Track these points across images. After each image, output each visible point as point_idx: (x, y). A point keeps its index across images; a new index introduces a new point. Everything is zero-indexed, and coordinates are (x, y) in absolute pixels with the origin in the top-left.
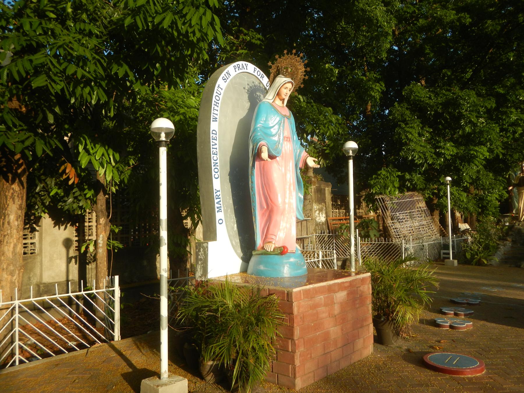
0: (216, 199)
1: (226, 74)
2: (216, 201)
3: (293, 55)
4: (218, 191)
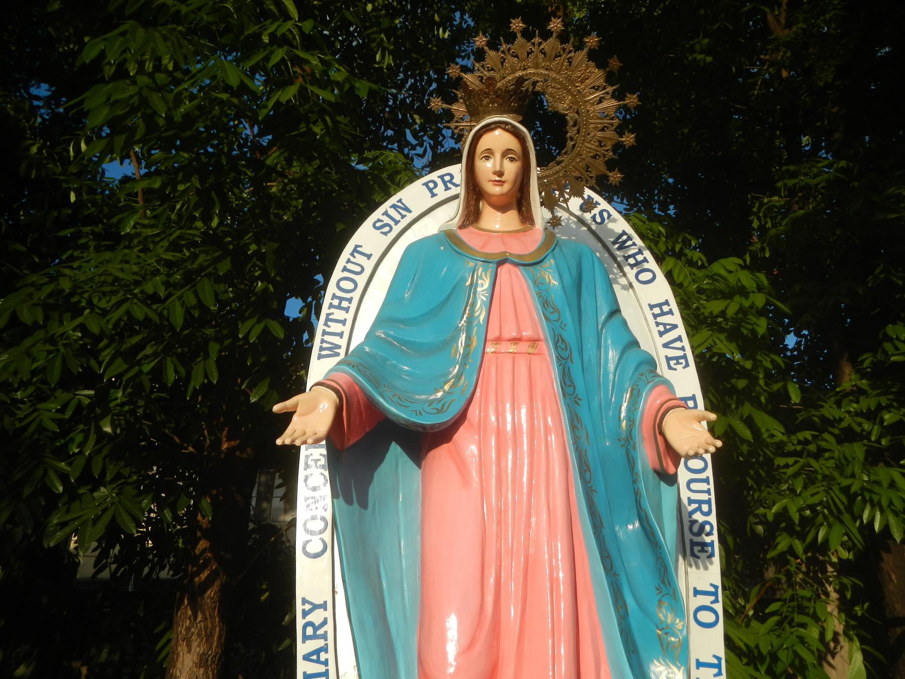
0: (305, 638)
1: (392, 212)
2: (302, 648)
3: (520, 39)
4: (315, 607)
